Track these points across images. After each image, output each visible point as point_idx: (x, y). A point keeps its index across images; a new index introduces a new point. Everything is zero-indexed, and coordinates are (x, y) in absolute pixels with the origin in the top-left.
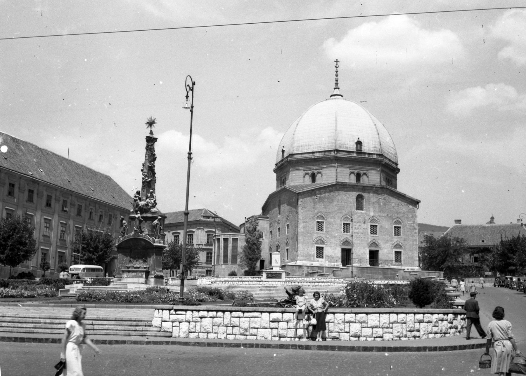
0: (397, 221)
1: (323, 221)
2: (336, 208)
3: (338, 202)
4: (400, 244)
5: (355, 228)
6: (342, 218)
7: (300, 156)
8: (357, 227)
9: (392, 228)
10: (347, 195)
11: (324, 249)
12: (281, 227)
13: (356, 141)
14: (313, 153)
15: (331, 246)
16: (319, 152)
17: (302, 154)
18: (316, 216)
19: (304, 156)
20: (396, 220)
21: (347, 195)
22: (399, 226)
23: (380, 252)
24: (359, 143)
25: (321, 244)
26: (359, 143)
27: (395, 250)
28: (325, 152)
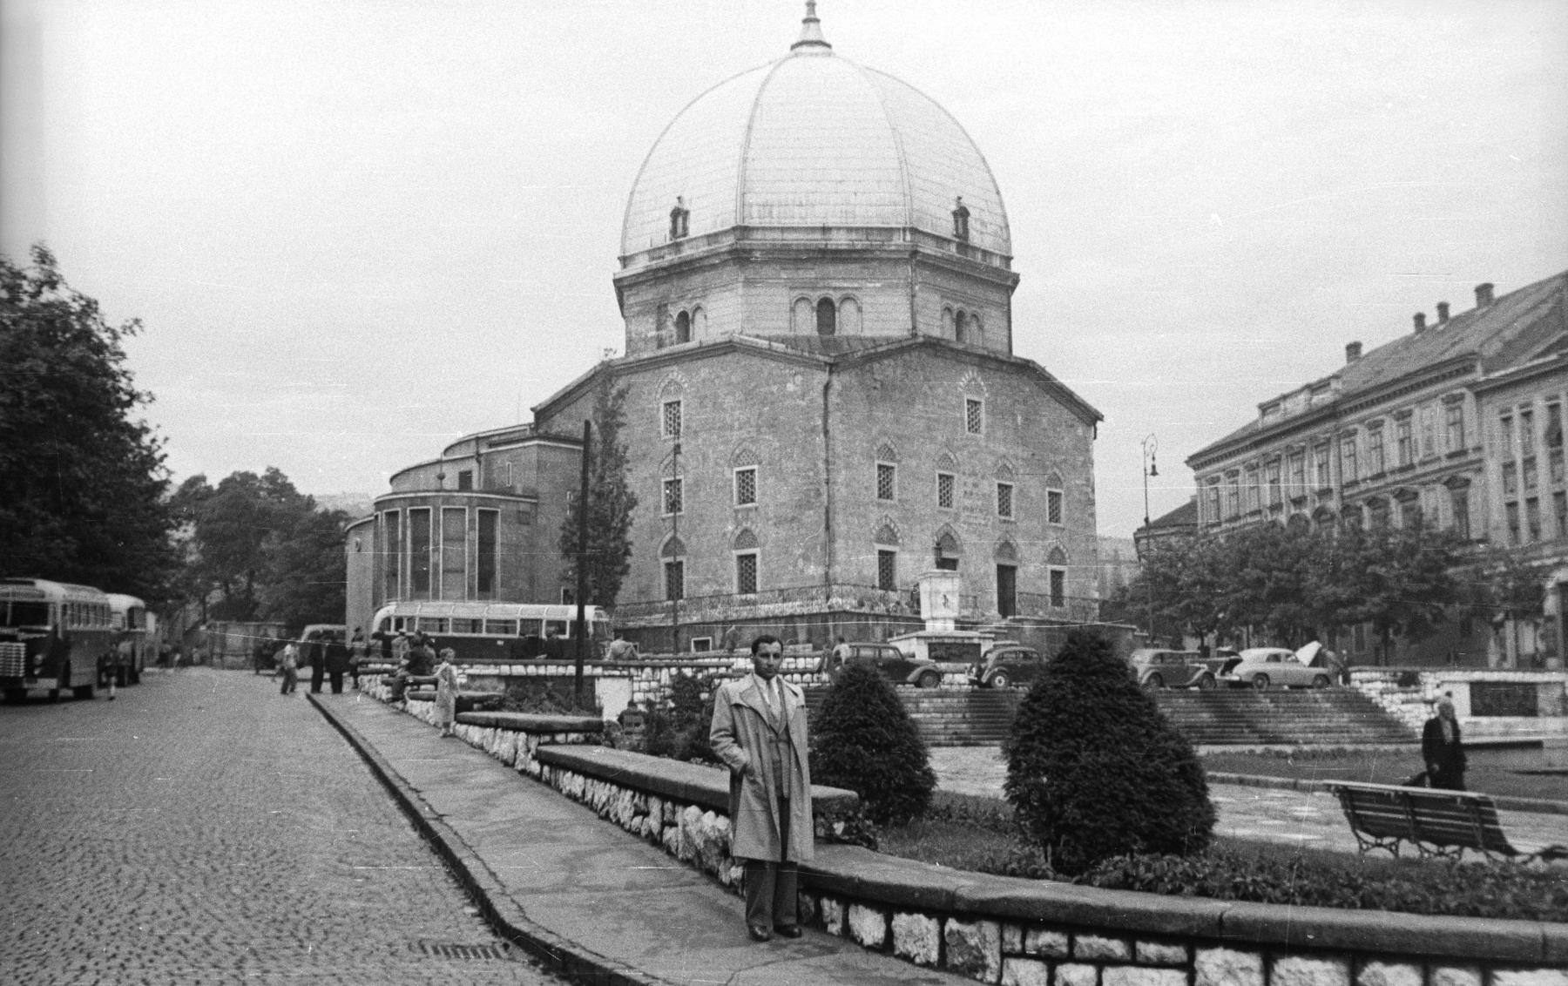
2: (922, 424)
3: (925, 404)
7: (777, 235)
8: (968, 490)
9: (1043, 497)
11: (897, 557)
13: (954, 207)
14: (825, 230)
15: (912, 551)
16: (850, 230)
17: (783, 230)
19: (791, 237)
20: (1050, 471)
22: (1057, 491)
23: (1020, 573)
24: (962, 214)
26: (962, 214)
28: (868, 230)
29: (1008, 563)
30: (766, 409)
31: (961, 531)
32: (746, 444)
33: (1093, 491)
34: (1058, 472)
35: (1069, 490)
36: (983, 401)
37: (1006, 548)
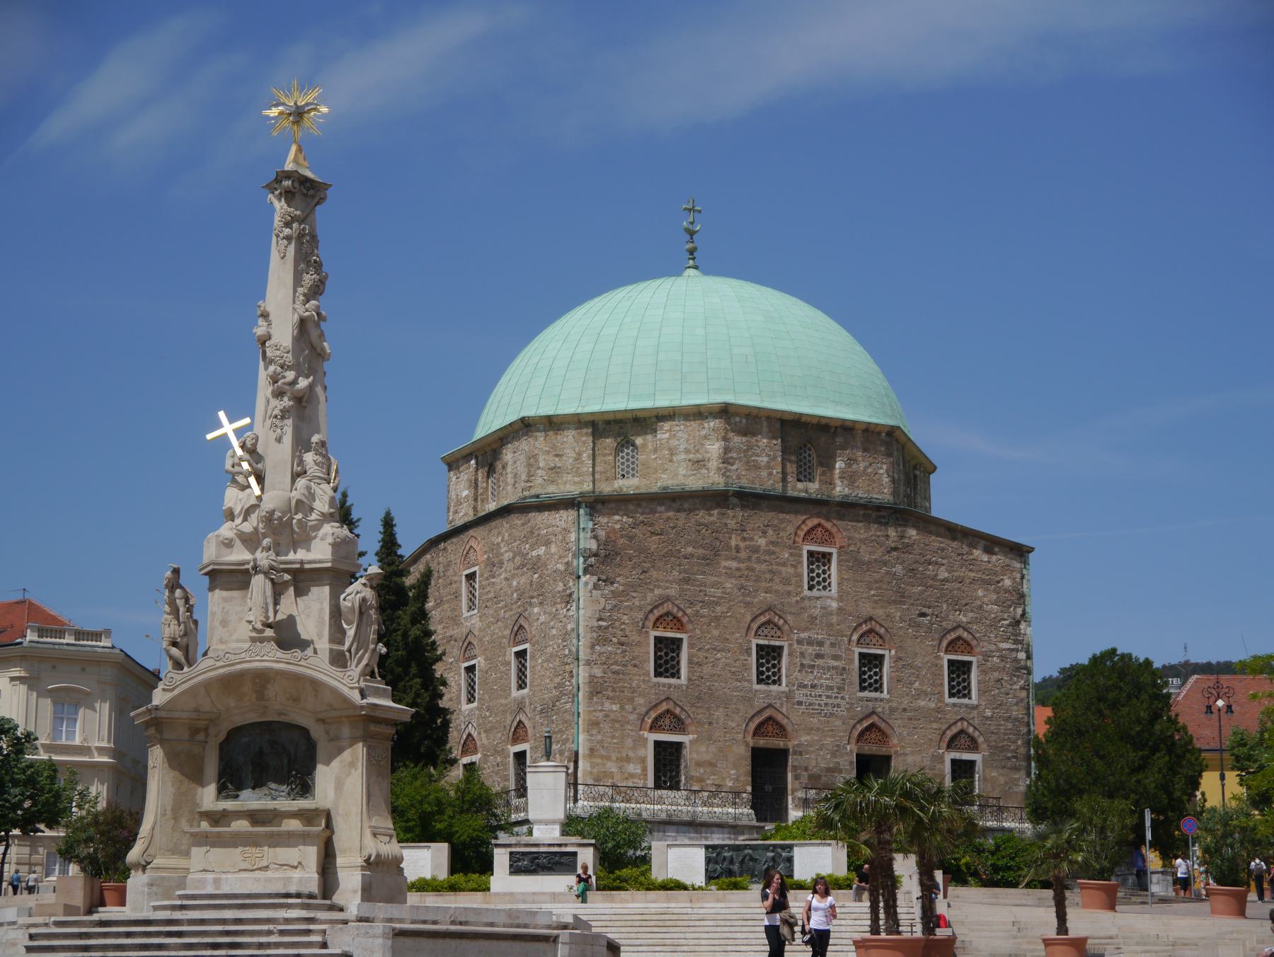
0: (959, 638)
1: (678, 635)
4: (971, 730)
5: (802, 665)
6: (755, 626)
10: (770, 532)
11: (686, 752)
12: (479, 662)
18: (652, 618)
20: (953, 636)
21: (770, 532)
25: (672, 730)
27: (950, 756)
29: (869, 749)
30: (536, 576)
31: (792, 717)
32: (522, 621)
33: (1029, 657)
34: (965, 635)
35: (987, 656)
36: (834, 551)
37: (873, 730)
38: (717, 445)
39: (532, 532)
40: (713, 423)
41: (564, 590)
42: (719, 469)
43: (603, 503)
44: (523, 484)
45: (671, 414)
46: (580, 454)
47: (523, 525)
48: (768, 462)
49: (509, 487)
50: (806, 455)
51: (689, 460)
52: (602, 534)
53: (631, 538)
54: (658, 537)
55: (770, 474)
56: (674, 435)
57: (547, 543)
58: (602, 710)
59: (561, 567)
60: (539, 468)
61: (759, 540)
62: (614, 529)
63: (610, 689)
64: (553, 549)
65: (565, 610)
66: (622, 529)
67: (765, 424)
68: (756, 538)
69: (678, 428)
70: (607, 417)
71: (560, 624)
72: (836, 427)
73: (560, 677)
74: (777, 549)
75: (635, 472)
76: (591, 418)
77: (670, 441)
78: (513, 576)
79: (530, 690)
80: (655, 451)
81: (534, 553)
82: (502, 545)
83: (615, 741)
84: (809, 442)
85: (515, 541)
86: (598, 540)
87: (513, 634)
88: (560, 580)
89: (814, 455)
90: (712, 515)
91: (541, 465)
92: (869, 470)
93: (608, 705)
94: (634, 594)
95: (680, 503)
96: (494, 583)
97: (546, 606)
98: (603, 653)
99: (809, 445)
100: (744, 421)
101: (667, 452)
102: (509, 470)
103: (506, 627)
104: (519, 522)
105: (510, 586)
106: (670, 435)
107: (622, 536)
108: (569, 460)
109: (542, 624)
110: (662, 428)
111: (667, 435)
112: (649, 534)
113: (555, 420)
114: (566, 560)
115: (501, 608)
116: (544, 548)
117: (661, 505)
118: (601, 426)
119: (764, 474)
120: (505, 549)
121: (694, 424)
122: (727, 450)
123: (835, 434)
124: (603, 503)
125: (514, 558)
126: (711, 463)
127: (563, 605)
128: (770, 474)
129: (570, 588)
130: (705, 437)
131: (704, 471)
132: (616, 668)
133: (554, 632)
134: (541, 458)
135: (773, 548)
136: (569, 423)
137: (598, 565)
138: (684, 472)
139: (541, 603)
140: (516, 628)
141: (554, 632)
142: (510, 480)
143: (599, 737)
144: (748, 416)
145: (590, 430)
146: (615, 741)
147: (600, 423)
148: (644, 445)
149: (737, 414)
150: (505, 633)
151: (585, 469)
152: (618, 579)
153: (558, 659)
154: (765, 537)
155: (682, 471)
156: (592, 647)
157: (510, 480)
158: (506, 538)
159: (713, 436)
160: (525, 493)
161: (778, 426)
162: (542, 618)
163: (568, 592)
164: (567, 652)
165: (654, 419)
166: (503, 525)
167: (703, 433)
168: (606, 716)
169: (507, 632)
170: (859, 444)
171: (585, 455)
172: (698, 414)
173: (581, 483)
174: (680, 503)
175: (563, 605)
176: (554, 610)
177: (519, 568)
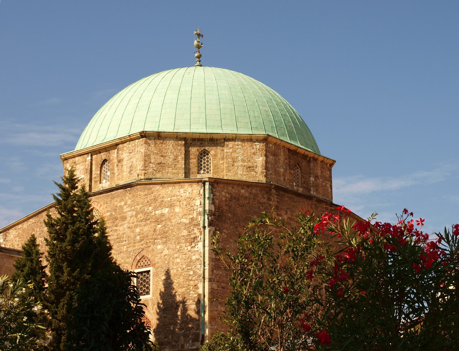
10: (289, 212)
30: (160, 226)
32: (144, 253)
38: (261, 159)
39: (155, 200)
40: (259, 146)
41: (188, 235)
42: (262, 173)
43: (217, 184)
44: (138, 172)
45: (234, 138)
46: (177, 156)
47: (145, 195)
48: (284, 173)
49: (125, 174)
50: (296, 171)
51: (244, 166)
52: (217, 202)
53: (230, 207)
54: (241, 208)
55: (285, 179)
56: (235, 150)
57: (171, 206)
58: (217, 310)
59: (184, 220)
60: (150, 163)
61: (284, 216)
62: (222, 200)
63: (221, 297)
64: (177, 209)
65: (189, 248)
66: (226, 201)
67: (282, 149)
68: (283, 214)
69: (237, 147)
70: (195, 137)
71: (184, 256)
72: (310, 157)
73: (184, 289)
74: (292, 222)
75: (209, 170)
76: (184, 136)
77: (232, 154)
78: (136, 226)
79: (153, 296)
80: (223, 159)
81: (157, 212)
82: (125, 207)
83: (223, 330)
84: (298, 164)
85: (138, 205)
86: (215, 206)
87: (136, 261)
88: (185, 229)
89: (300, 172)
90: (264, 198)
91: (152, 161)
92: (324, 184)
93: (219, 307)
94: (231, 241)
95: (251, 189)
96: (116, 230)
97: (170, 245)
98: (218, 275)
99: (298, 166)
100: (273, 147)
101: (230, 160)
102: (124, 163)
103: (128, 258)
104: (142, 193)
105: (133, 232)
106: (233, 151)
107: (226, 205)
108: (170, 159)
109: (165, 255)
110: (227, 146)
111: (231, 150)
112: (237, 206)
113: (162, 135)
114: (191, 216)
115: (124, 245)
116: (167, 210)
117: (243, 188)
118: (189, 142)
119: (282, 179)
120: (128, 209)
121: (247, 145)
122: (266, 162)
123: (309, 161)
124: (217, 184)
125: (136, 216)
126: (257, 169)
127: (188, 244)
128: (285, 179)
129: (195, 234)
130: (254, 154)
131: (253, 173)
132: (223, 285)
133: (178, 260)
134: (152, 157)
135: (290, 222)
136: (170, 138)
137: (215, 221)
138: (241, 173)
139: (165, 243)
140: (138, 258)
141: (178, 260)
142: (126, 169)
143: (216, 327)
144: (275, 144)
145: (183, 142)
146: (223, 330)
147: (190, 139)
148: (215, 156)
149: (270, 142)
150: (127, 260)
151: (180, 166)
152: (224, 231)
153: (182, 277)
154: (287, 215)
155: (240, 172)
156: (212, 271)
157: (126, 169)
158: (129, 202)
159: (259, 153)
160: (140, 177)
161: (287, 152)
162: (166, 252)
163: (192, 236)
164: (191, 273)
165: (223, 141)
166: (128, 196)
167: (253, 151)
168: (219, 314)
169: (130, 260)
170: (319, 169)
171: (180, 157)
172: (250, 139)
173: (178, 173)
174: (251, 189)
175: (188, 244)
176: (178, 247)
177: (142, 221)
